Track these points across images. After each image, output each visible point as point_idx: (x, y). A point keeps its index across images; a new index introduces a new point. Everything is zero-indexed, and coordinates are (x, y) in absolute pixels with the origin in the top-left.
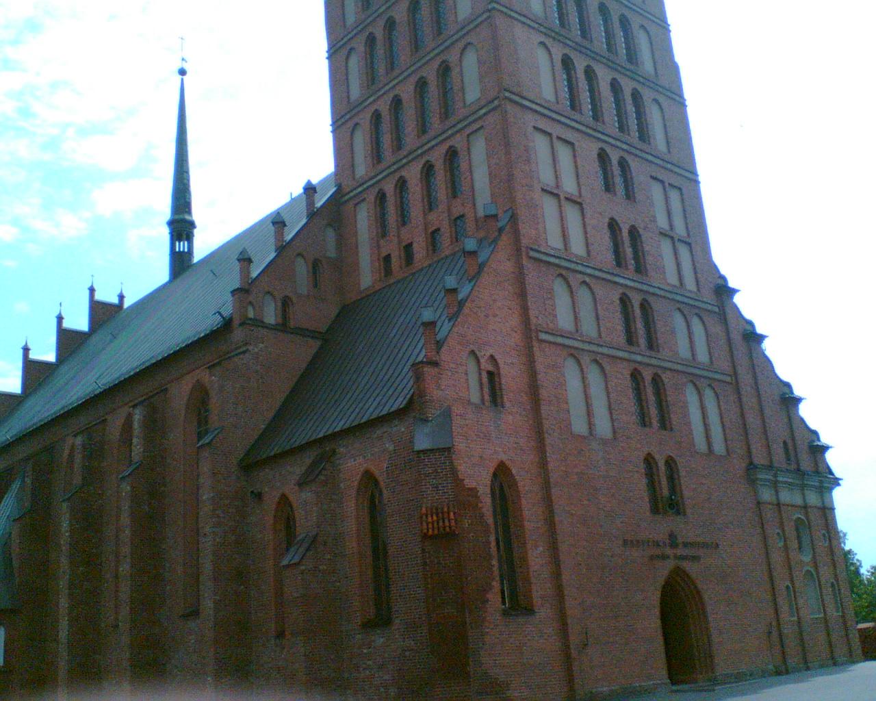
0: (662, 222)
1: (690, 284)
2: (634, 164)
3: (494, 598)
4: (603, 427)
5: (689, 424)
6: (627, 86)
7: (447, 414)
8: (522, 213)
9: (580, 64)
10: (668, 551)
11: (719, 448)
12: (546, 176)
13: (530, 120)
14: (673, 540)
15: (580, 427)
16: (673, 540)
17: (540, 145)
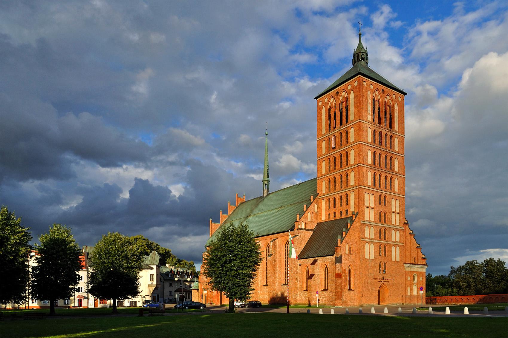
0: (393, 210)
1: (398, 224)
2: (388, 197)
3: (347, 288)
4: (372, 257)
5: (391, 255)
6: (389, 176)
7: (341, 256)
8: (360, 213)
9: (378, 174)
10: (382, 280)
11: (398, 260)
12: (367, 204)
13: (364, 191)
14: (383, 279)
15: (367, 257)
16: (383, 279)
17: (366, 196)
